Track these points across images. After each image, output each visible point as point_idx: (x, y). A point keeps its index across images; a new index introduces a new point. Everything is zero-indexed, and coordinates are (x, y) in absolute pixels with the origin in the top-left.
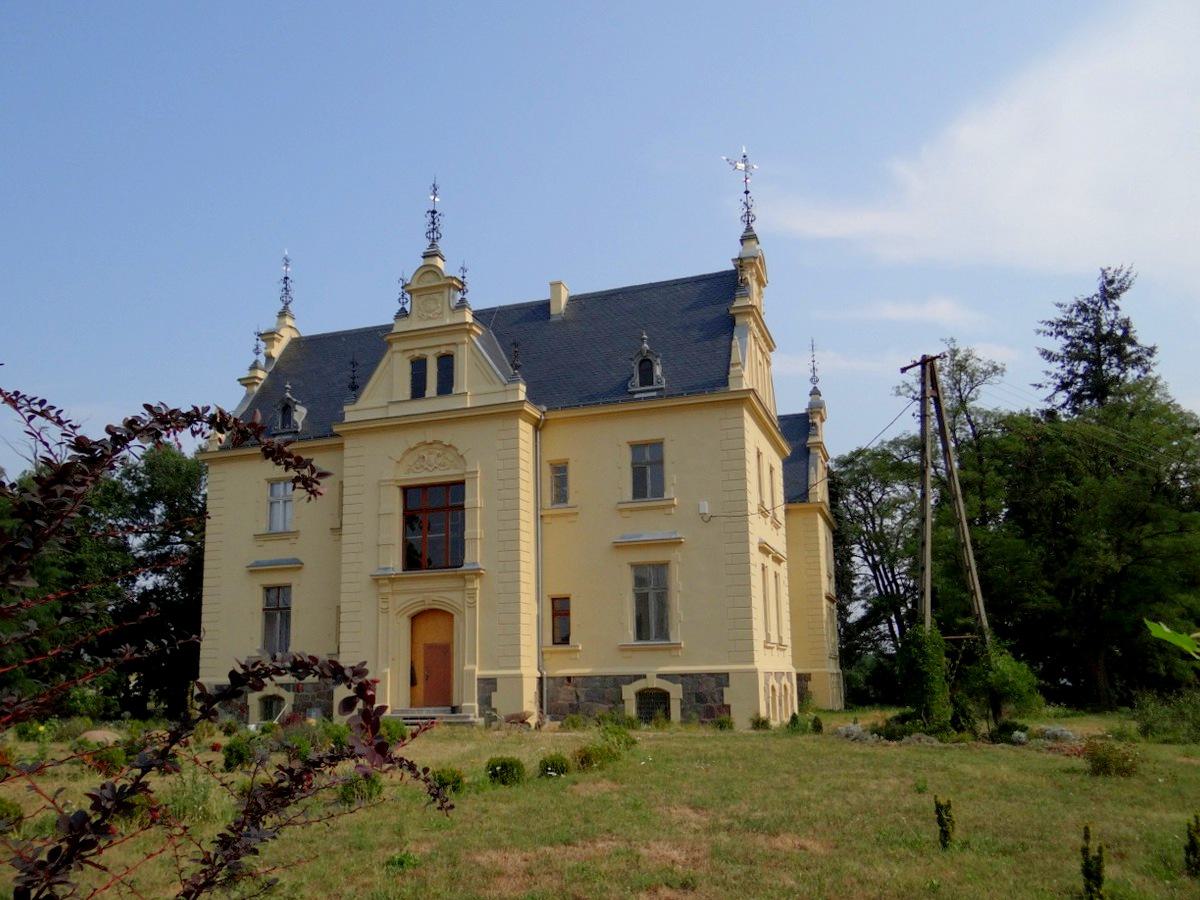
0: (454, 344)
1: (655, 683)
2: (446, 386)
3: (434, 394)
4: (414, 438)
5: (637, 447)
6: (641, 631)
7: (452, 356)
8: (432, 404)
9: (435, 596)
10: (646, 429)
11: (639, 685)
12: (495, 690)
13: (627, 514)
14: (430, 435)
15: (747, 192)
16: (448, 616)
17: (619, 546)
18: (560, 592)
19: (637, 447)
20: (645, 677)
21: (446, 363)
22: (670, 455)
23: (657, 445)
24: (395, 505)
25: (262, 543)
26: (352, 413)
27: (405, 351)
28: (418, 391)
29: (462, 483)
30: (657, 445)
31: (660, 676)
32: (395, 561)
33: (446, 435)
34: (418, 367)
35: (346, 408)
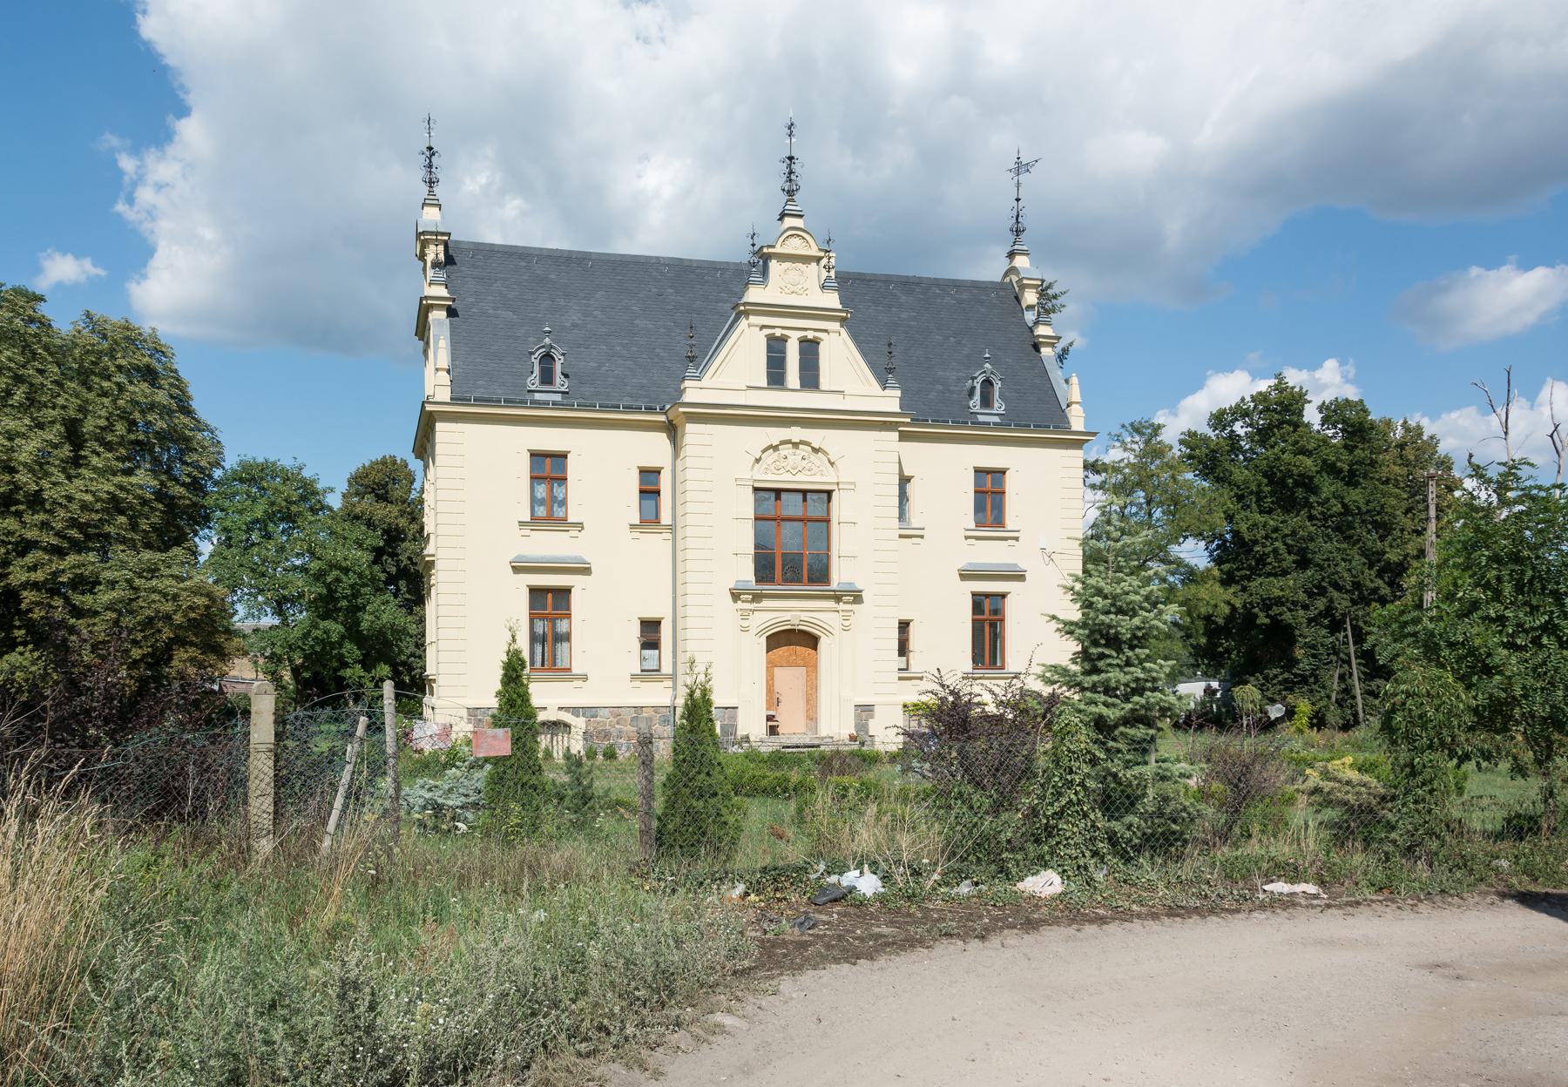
0: (826, 331)
2: (810, 379)
4: (776, 434)
6: (977, 658)
7: (818, 343)
8: (793, 398)
9: (804, 616)
10: (991, 456)
12: (872, 717)
13: (973, 541)
14: (796, 433)
15: (1018, 200)
16: (811, 641)
17: (966, 576)
18: (905, 617)
21: (810, 349)
22: (1011, 484)
24: (746, 505)
25: (528, 532)
26: (694, 393)
27: (763, 327)
28: (776, 376)
29: (829, 493)
32: (746, 572)
33: (815, 436)
34: (776, 347)
35: (687, 383)
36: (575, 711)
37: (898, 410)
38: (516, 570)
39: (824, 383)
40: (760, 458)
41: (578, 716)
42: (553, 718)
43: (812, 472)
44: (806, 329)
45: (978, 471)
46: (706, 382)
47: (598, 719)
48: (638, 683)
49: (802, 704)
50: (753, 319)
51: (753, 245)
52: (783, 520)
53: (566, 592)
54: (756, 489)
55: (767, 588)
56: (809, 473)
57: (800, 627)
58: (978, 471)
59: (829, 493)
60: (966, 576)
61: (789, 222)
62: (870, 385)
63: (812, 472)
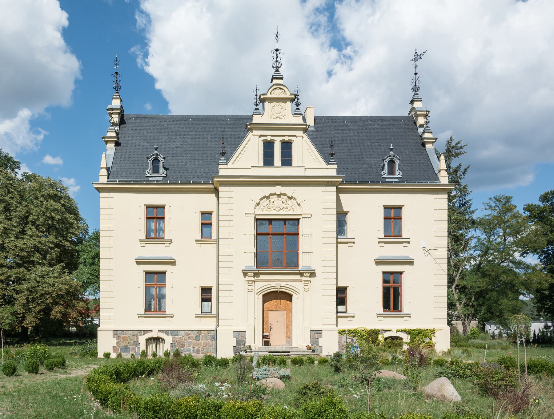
0: (295, 136)
1: (394, 334)
2: (287, 161)
3: (280, 165)
4: (267, 190)
5: (387, 208)
6: (386, 306)
7: (292, 143)
9: (283, 284)
11: (387, 335)
12: (321, 337)
13: (383, 244)
14: (278, 189)
16: (288, 297)
17: (379, 262)
19: (387, 208)
20: (390, 331)
21: (287, 146)
22: (405, 214)
23: (399, 208)
26: (224, 170)
27: (260, 136)
28: (268, 161)
29: (298, 220)
30: (399, 208)
31: (398, 331)
32: (251, 262)
34: (268, 146)
36: (167, 332)
37: (335, 174)
38: (138, 263)
39: (294, 163)
40: (259, 203)
41: (168, 335)
42: (155, 336)
43: (288, 209)
44: (284, 136)
45: (386, 208)
46: (230, 165)
47: (179, 336)
48: (199, 319)
49: (284, 330)
50: (255, 132)
51: (256, 95)
52: (273, 235)
53: (164, 273)
54: (257, 220)
55: (262, 270)
56: (286, 210)
57: (281, 290)
58: (386, 208)
59: (298, 220)
60: (379, 262)
61: (275, 81)
62: (320, 163)
63: (288, 209)
